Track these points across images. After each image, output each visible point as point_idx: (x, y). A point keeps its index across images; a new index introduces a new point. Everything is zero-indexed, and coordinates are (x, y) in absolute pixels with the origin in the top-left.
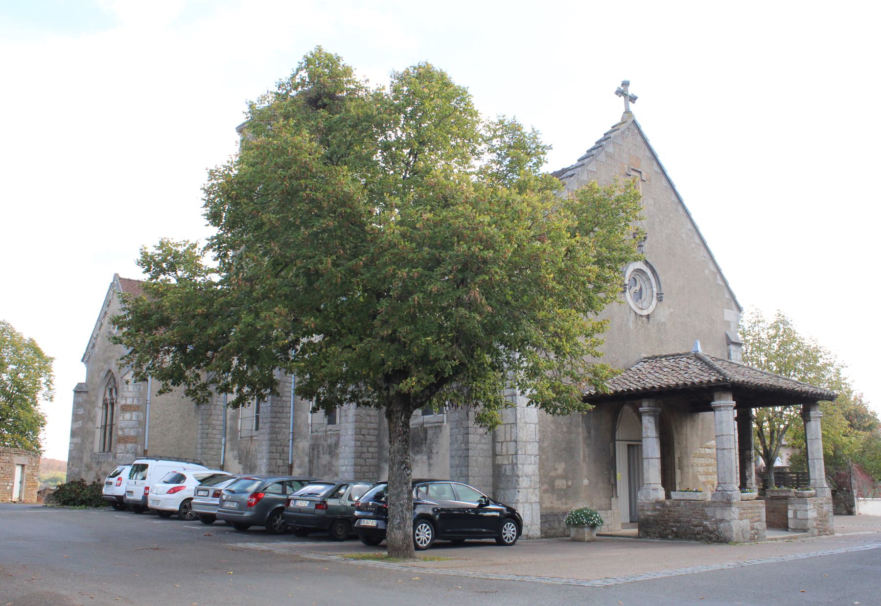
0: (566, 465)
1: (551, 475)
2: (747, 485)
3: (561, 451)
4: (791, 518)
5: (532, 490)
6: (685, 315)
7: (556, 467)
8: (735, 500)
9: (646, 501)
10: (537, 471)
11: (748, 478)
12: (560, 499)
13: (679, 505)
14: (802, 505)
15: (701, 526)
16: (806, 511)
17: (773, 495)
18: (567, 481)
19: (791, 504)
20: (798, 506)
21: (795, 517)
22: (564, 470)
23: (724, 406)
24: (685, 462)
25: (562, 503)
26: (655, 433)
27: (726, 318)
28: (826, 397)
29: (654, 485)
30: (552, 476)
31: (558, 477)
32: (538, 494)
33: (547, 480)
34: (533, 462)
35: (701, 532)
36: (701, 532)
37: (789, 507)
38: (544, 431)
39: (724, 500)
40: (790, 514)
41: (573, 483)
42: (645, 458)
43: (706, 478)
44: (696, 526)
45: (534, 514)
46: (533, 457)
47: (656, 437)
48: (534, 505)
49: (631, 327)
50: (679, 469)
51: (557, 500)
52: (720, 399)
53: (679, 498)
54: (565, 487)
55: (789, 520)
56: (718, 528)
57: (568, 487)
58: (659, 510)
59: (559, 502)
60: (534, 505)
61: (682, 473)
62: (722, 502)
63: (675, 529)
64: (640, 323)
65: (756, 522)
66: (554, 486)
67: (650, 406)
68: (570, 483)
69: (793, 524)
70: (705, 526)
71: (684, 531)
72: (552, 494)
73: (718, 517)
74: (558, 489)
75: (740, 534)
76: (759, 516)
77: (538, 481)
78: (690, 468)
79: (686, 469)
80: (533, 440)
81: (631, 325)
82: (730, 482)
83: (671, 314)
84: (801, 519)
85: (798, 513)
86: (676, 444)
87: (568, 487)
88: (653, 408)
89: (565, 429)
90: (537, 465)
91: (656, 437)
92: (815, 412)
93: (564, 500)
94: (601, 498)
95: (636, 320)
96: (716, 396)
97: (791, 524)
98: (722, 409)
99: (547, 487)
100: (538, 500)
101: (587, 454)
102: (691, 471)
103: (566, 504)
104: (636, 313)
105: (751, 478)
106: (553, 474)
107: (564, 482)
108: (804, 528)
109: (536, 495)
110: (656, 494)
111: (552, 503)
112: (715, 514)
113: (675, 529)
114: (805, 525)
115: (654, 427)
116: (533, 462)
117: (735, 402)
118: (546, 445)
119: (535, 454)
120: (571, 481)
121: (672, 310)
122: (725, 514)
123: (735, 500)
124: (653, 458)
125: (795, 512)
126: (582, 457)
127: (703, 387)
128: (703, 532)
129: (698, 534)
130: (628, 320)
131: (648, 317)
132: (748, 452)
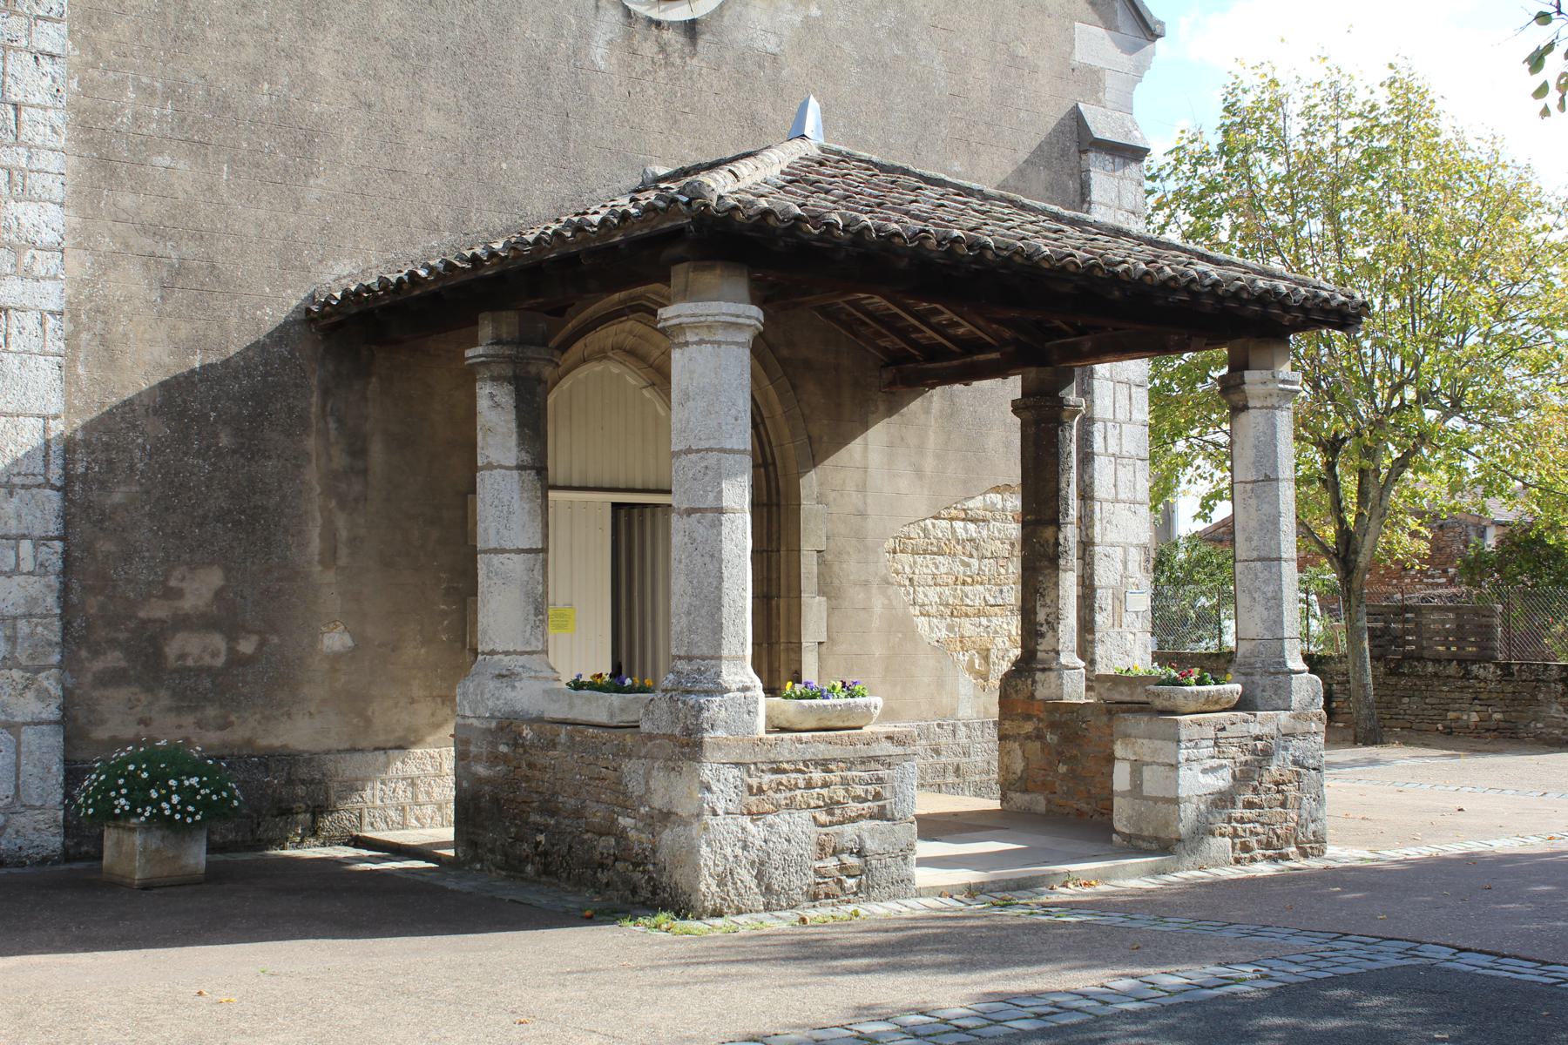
0: (227, 579)
1: (142, 614)
2: (1040, 655)
3: (200, 525)
4: (1123, 795)
5: (16, 674)
6: (881, 35)
7: (173, 583)
8: (720, 733)
9: (476, 722)
10: (51, 601)
11: (1044, 629)
12: (193, 709)
13: (553, 745)
14: (1159, 743)
15: (608, 834)
16: (1175, 767)
17: (1118, 697)
18: (232, 639)
19: (1126, 736)
20: (1144, 748)
21: (1136, 788)
22: (219, 594)
23: (694, 327)
24: (851, 568)
25: (200, 724)
26: (515, 450)
27: (1080, 57)
28: (1302, 308)
29: (507, 659)
30: (144, 623)
31: (183, 622)
32: (55, 690)
33: (122, 636)
34: (27, 565)
35: (609, 862)
36: (609, 862)
37: (1119, 750)
38: (107, 447)
39: (677, 732)
40: (1121, 777)
41: (262, 644)
42: (485, 552)
43: (950, 628)
44: (601, 835)
45: (27, 768)
46: (26, 547)
47: (520, 467)
48: (28, 735)
49: (602, 64)
50: (821, 592)
51: (178, 710)
52: (687, 295)
53: (560, 716)
54: (220, 662)
55: (1117, 801)
56: (654, 851)
57: (237, 661)
58: (505, 759)
59: (189, 720)
60: (28, 735)
61: (832, 610)
62: (671, 737)
63: (541, 838)
64: (649, 49)
65: (853, 820)
66: (159, 654)
67: (498, 342)
68: (247, 646)
69: (1129, 818)
70: (621, 836)
71: (565, 849)
72: (149, 690)
73: (658, 802)
74: (183, 672)
75: (746, 876)
76: (877, 796)
77: (58, 639)
78: (874, 590)
79: (856, 595)
80: (30, 481)
81: (599, 53)
82: (705, 651)
83: (808, 23)
84: (1156, 800)
85: (1147, 772)
86: (806, 504)
87: (237, 661)
88: (507, 351)
89: (224, 440)
90: (53, 580)
91: (520, 467)
92: (1266, 374)
93: (211, 712)
94: (413, 701)
95: (629, 36)
96: (679, 274)
97: (1121, 821)
98: (691, 337)
99: (123, 664)
100: (51, 712)
101: (344, 534)
102: (878, 604)
103: (225, 725)
104: (628, 13)
105: (1055, 630)
106: (158, 610)
107: (218, 642)
108: (1162, 835)
109: (43, 694)
110: (509, 694)
111: (144, 722)
112: (648, 790)
113: (541, 838)
114: (1167, 825)
115: (513, 425)
116: (27, 565)
117: (755, 311)
118: (118, 497)
119: (38, 532)
120: (255, 639)
121: (814, 11)
122: (662, 789)
123: (720, 733)
124: (503, 551)
125: (1137, 767)
126: (315, 545)
127: (615, 246)
128: (616, 860)
129: (602, 866)
130: (585, 35)
131: (691, 29)
132: (1049, 532)
